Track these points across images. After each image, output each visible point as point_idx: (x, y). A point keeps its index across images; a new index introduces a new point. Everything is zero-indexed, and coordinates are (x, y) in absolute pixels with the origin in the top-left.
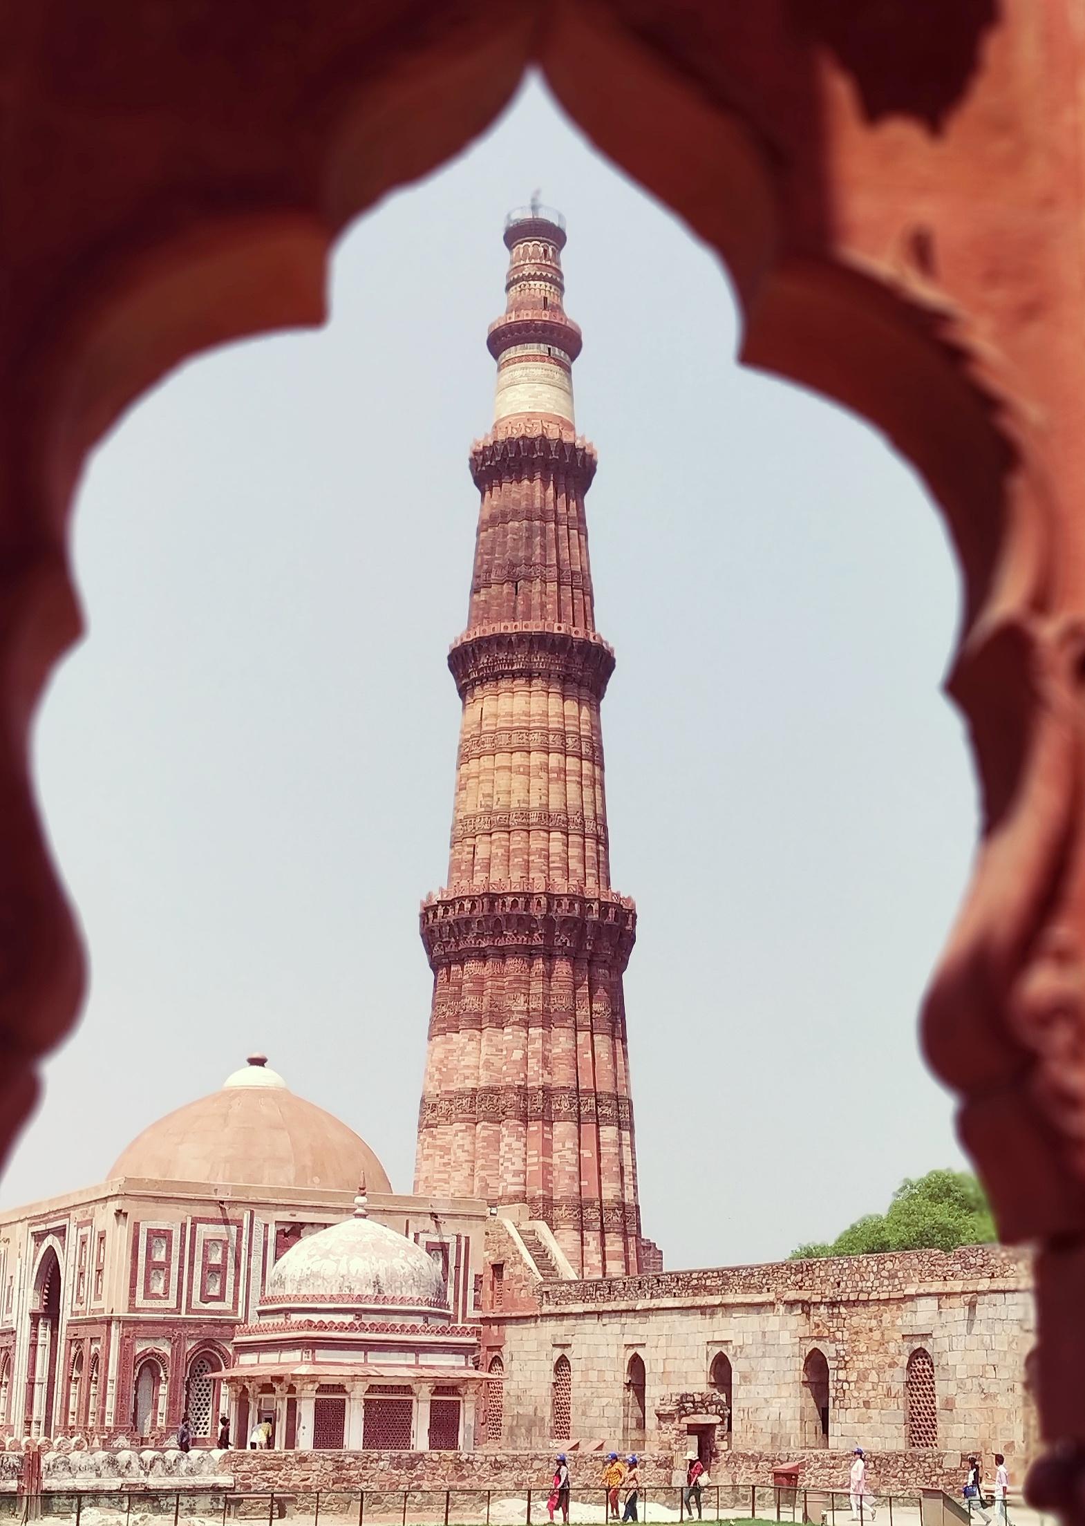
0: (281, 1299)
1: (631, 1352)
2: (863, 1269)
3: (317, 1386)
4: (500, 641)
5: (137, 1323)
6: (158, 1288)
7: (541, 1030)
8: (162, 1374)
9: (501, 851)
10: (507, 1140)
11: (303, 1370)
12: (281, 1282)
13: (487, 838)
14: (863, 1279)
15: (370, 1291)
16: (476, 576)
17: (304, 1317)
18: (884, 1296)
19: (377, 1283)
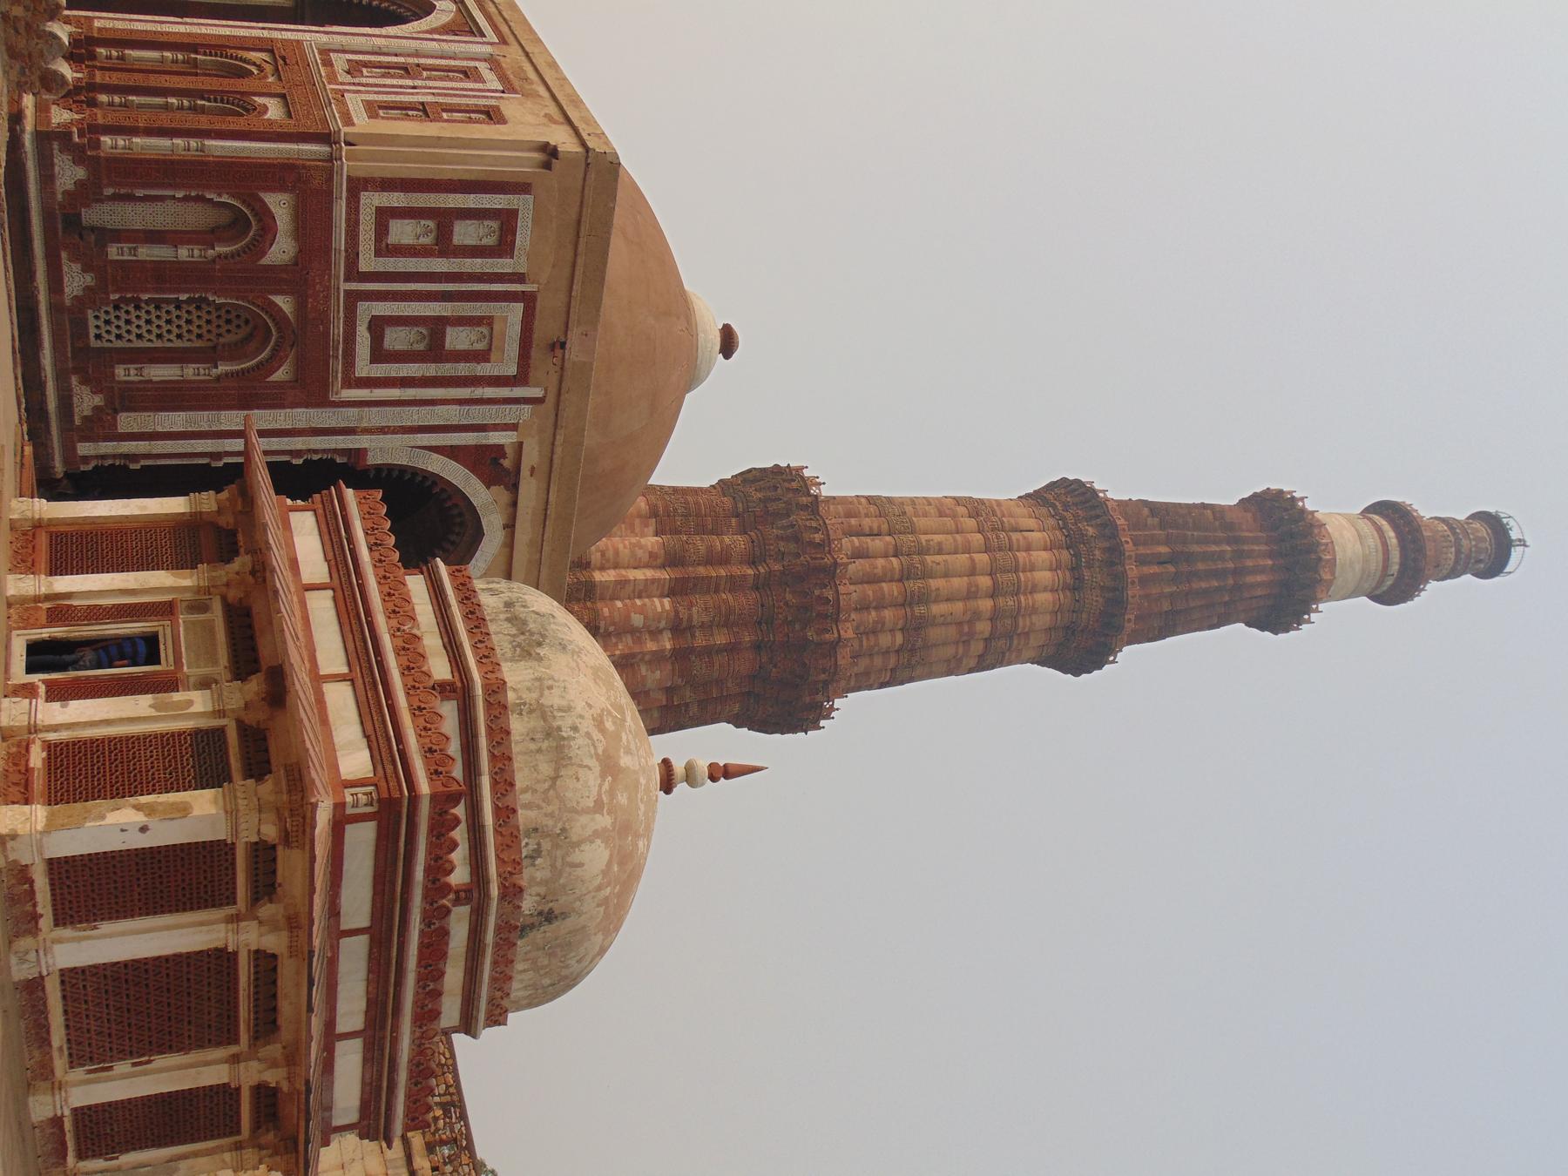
0: (487, 656)
5: (328, 196)
6: (403, 233)
7: (668, 646)
9: (879, 571)
12: (530, 644)
13: (891, 551)
15: (528, 904)
19: (549, 917)
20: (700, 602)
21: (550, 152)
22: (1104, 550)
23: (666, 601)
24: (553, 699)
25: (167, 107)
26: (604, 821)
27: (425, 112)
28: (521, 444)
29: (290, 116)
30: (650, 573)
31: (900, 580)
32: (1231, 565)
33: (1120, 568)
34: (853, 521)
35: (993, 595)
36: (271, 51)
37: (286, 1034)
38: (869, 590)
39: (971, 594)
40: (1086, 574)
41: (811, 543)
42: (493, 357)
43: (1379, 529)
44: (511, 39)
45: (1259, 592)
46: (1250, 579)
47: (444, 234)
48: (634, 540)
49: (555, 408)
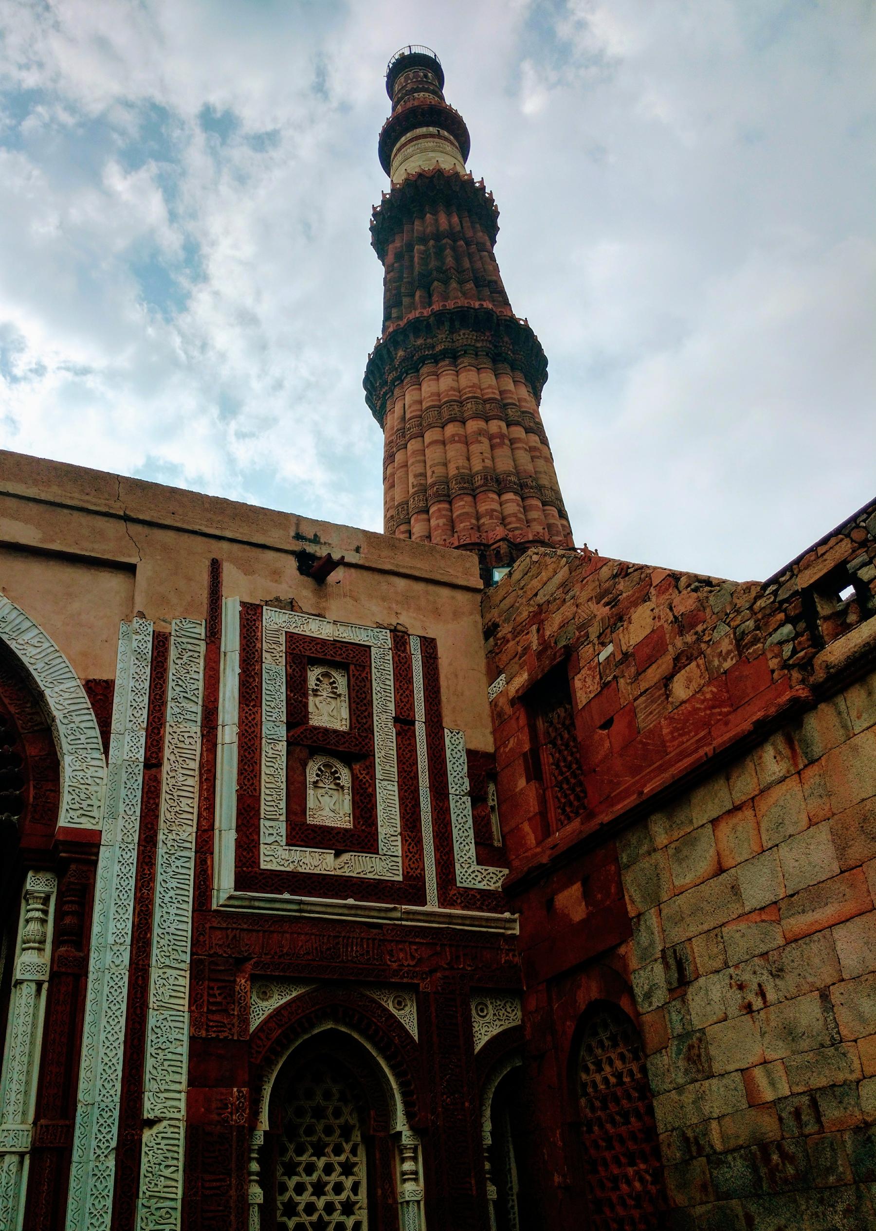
9: (441, 522)
13: (425, 516)
22: (417, 337)
31: (450, 503)
43: (399, 150)
45: (455, 219)
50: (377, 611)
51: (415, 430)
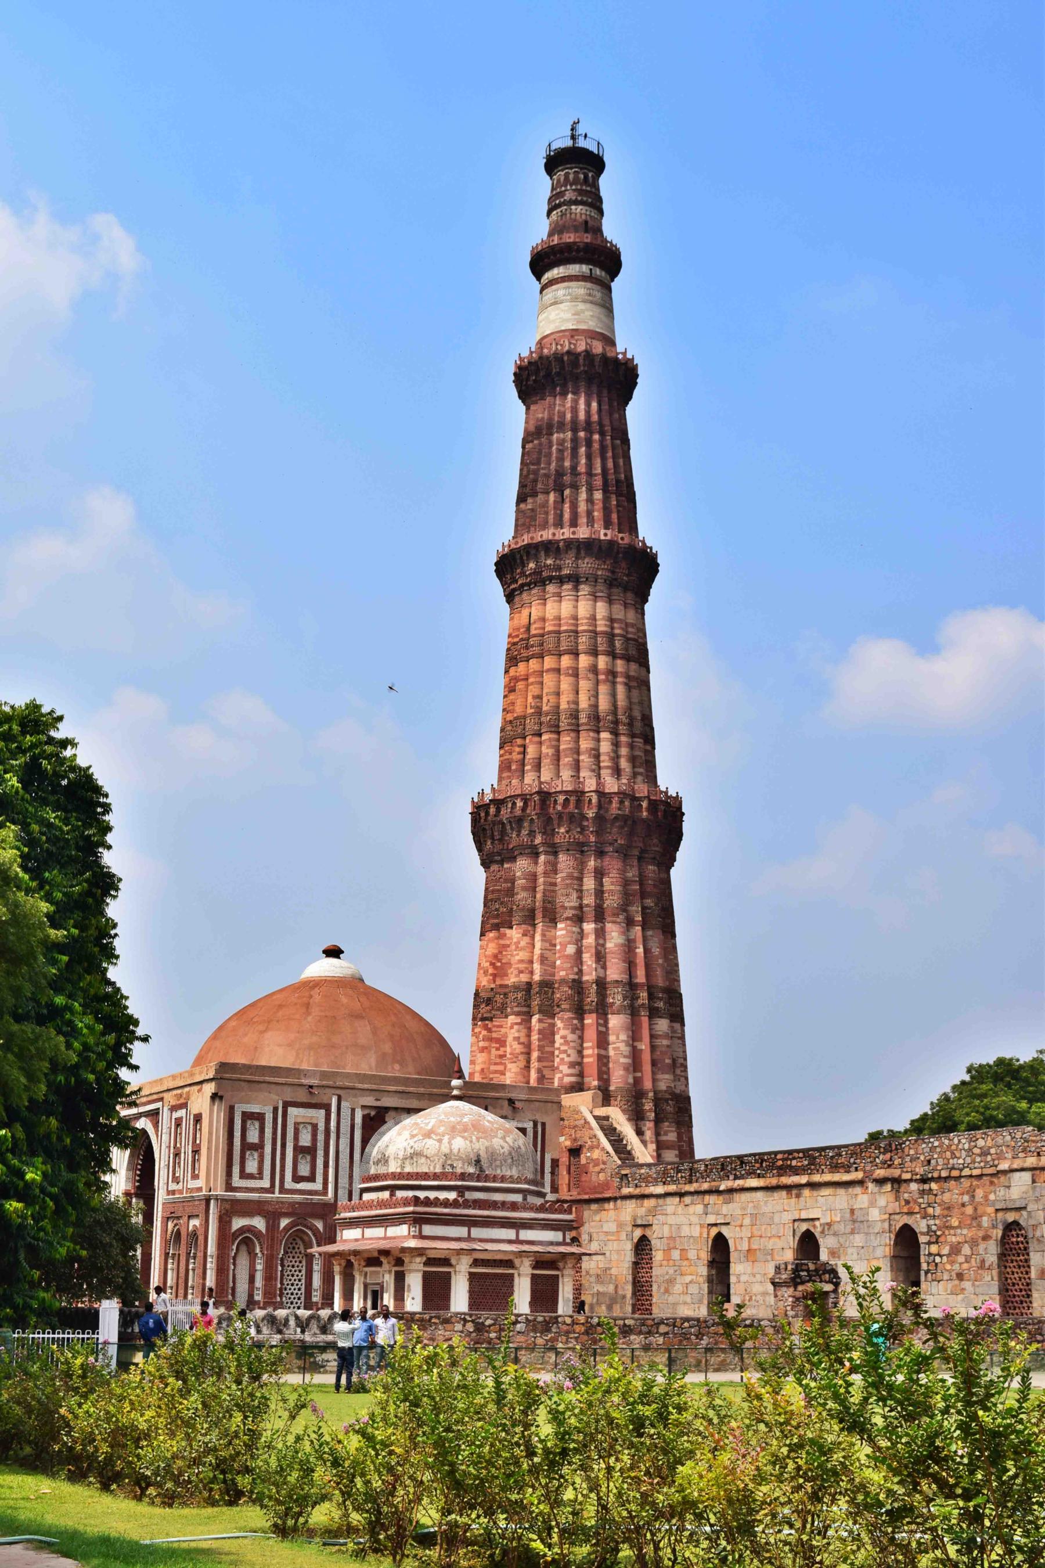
0: (385, 1177)
1: (714, 1231)
2: (954, 1147)
3: (424, 1259)
4: (549, 547)
5: (235, 1202)
6: (252, 1167)
7: (592, 926)
8: (258, 1250)
9: (551, 751)
10: (562, 1032)
11: (412, 1243)
12: (384, 1160)
13: (537, 739)
14: (954, 1156)
15: (471, 1170)
16: (522, 485)
17: (410, 1194)
18: (976, 1172)
19: (478, 1161)
20: (562, 899)
21: (214, 1097)
22: (547, 556)
23: (560, 926)
24: (401, 1155)
25: (193, 1270)
26: (446, 1139)
27: (196, 1151)
28: (363, 1107)
29: (198, 1216)
30: (538, 937)
31: (558, 733)
32: (569, 434)
33: (561, 544)
34: (513, 767)
35: (576, 654)
36: (168, 1218)
37: (511, 1257)
38: (566, 760)
39: (575, 674)
40: (566, 571)
41: (524, 809)
42: (315, 1122)
44: (161, 1095)
46: (582, 416)
47: (254, 1147)
48: (513, 947)
49: (342, 1091)
50: (530, 1116)
51: (536, 650)
